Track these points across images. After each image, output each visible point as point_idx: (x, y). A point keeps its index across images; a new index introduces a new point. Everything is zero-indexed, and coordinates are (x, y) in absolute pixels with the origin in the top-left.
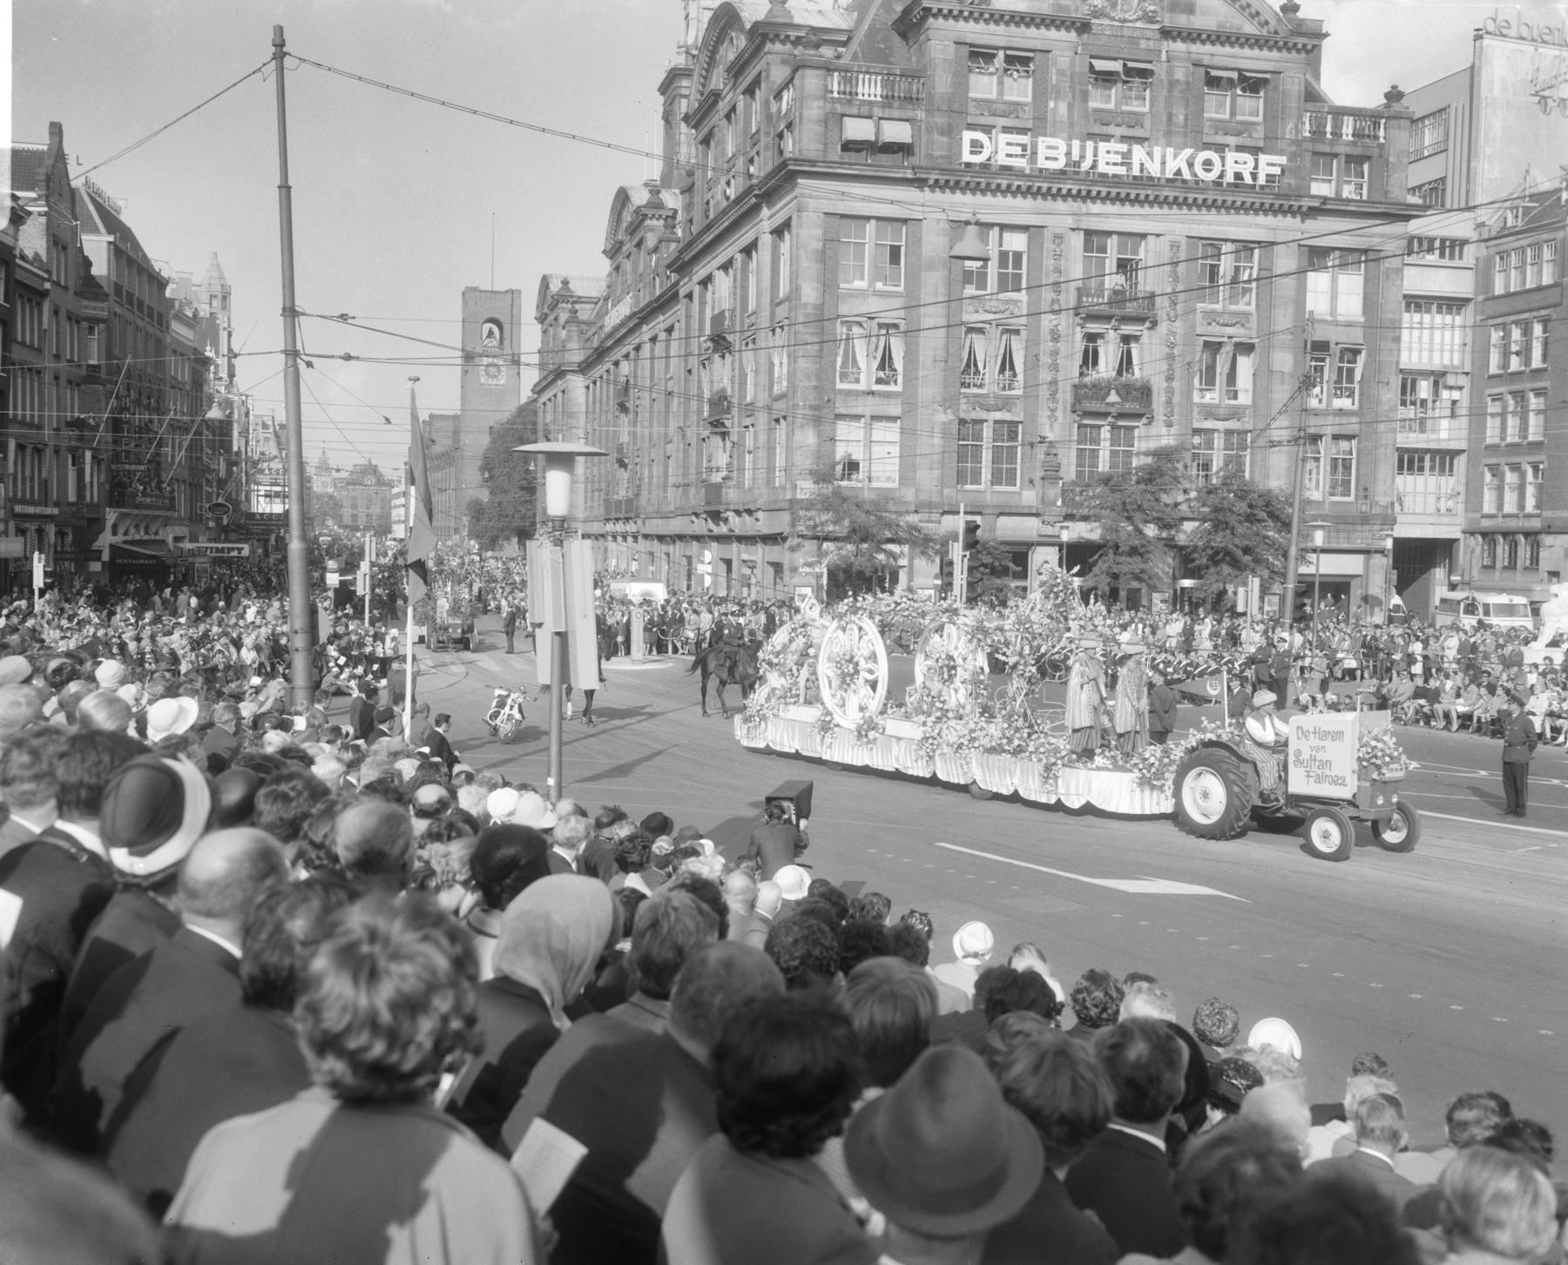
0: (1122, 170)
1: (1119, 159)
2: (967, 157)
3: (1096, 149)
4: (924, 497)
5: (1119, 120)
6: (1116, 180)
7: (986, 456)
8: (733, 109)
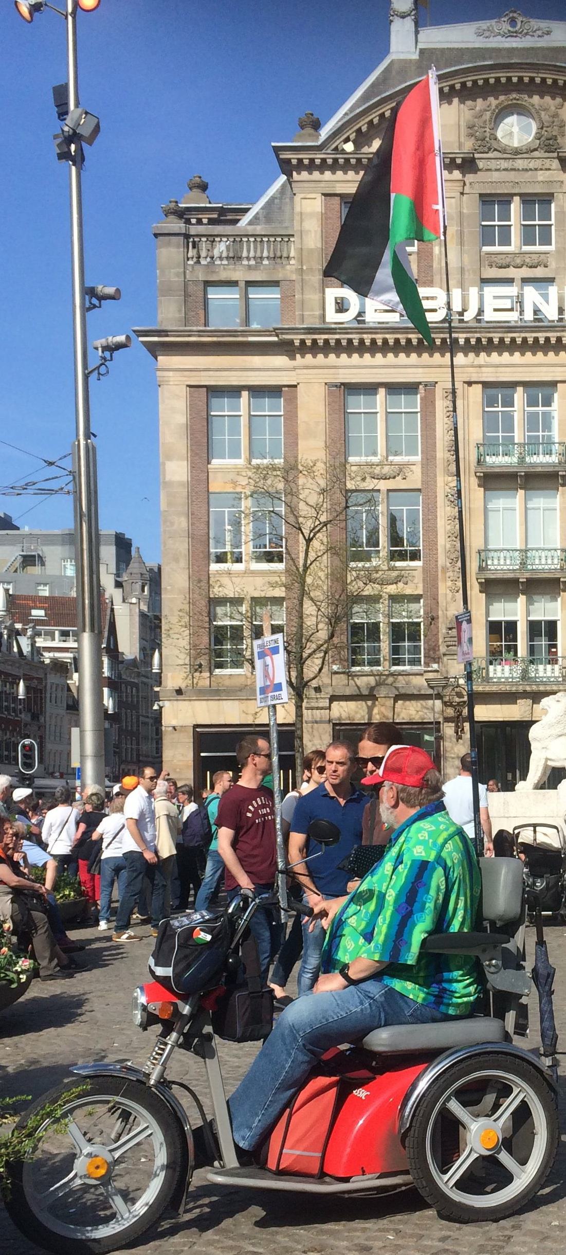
0: (513, 317)
1: (507, 304)
2: (332, 316)
3: (481, 298)
5: (518, 261)
6: (509, 328)
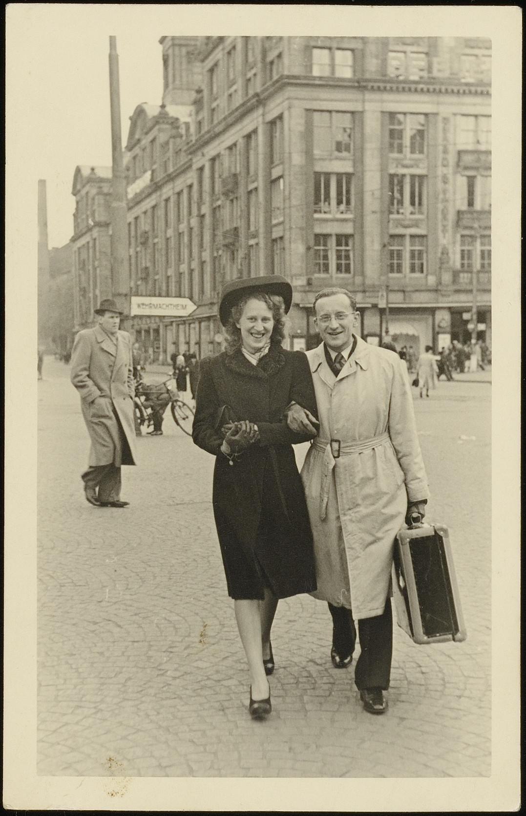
4: (368, 282)
7: (407, 256)
8: (234, 48)
